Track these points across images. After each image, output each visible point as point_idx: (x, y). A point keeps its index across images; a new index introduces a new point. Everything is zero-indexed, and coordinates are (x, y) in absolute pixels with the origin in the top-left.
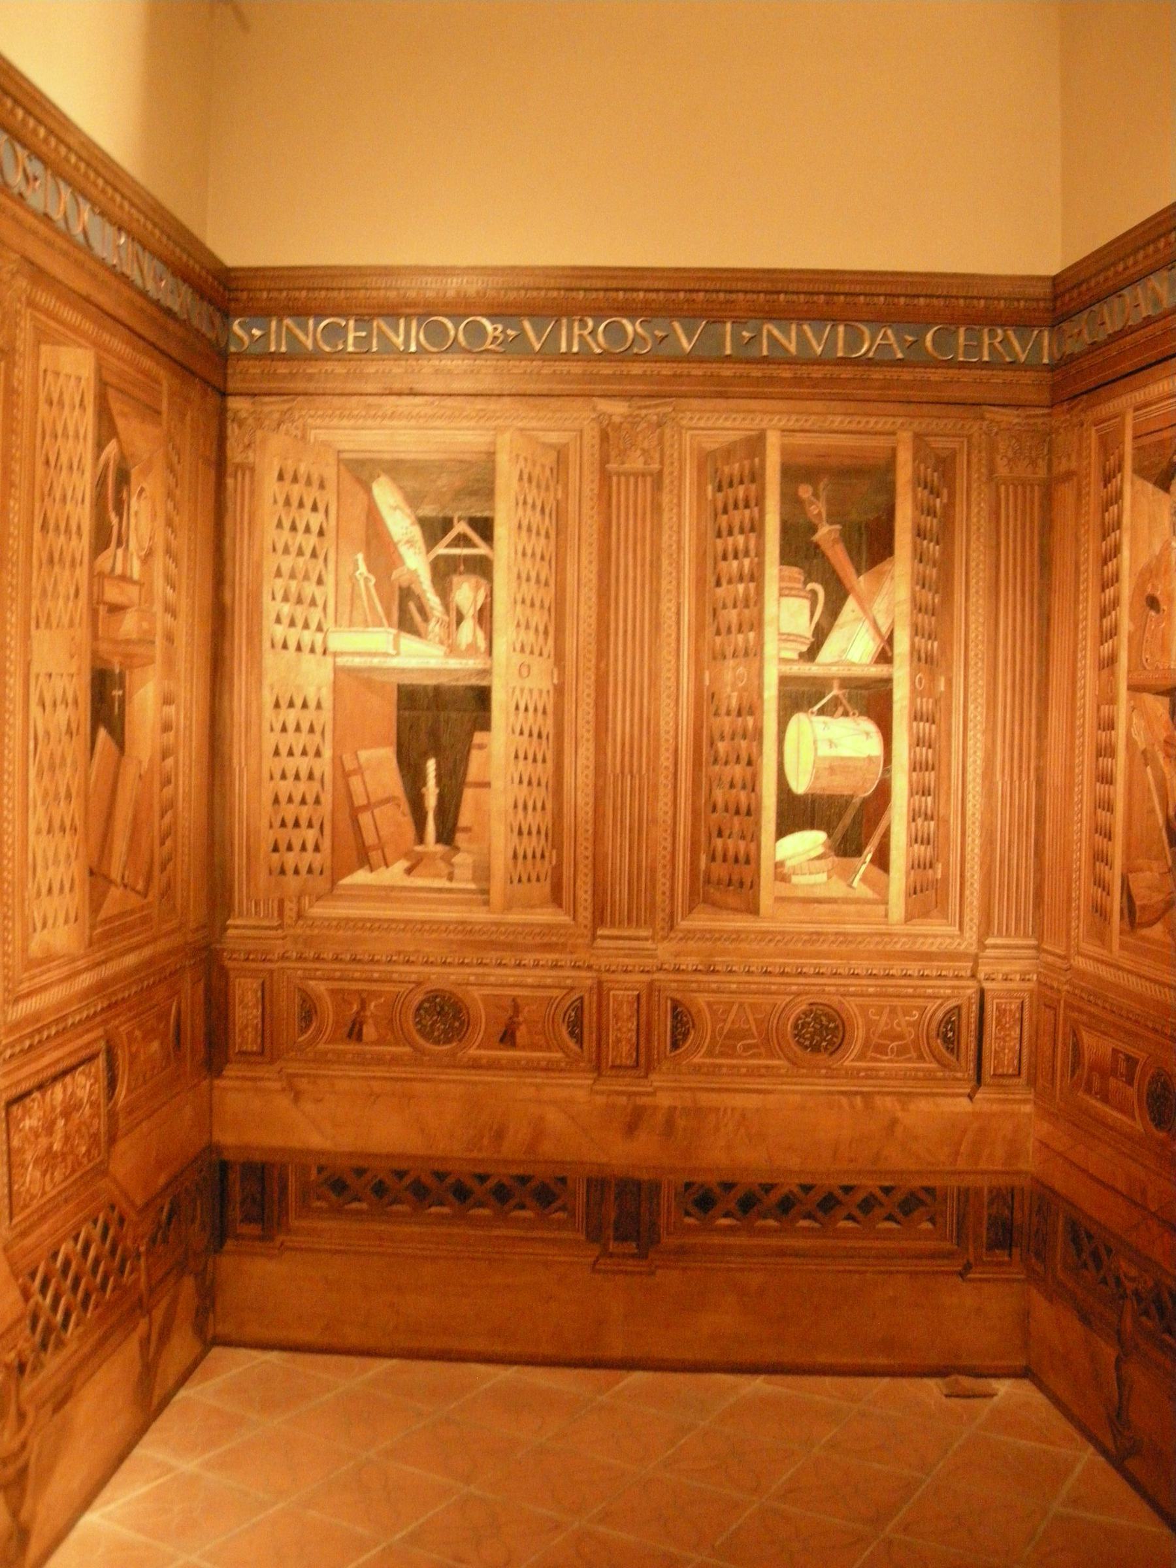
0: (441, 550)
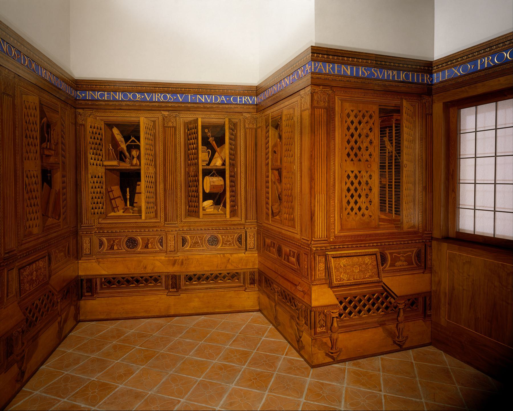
0: (128, 143)
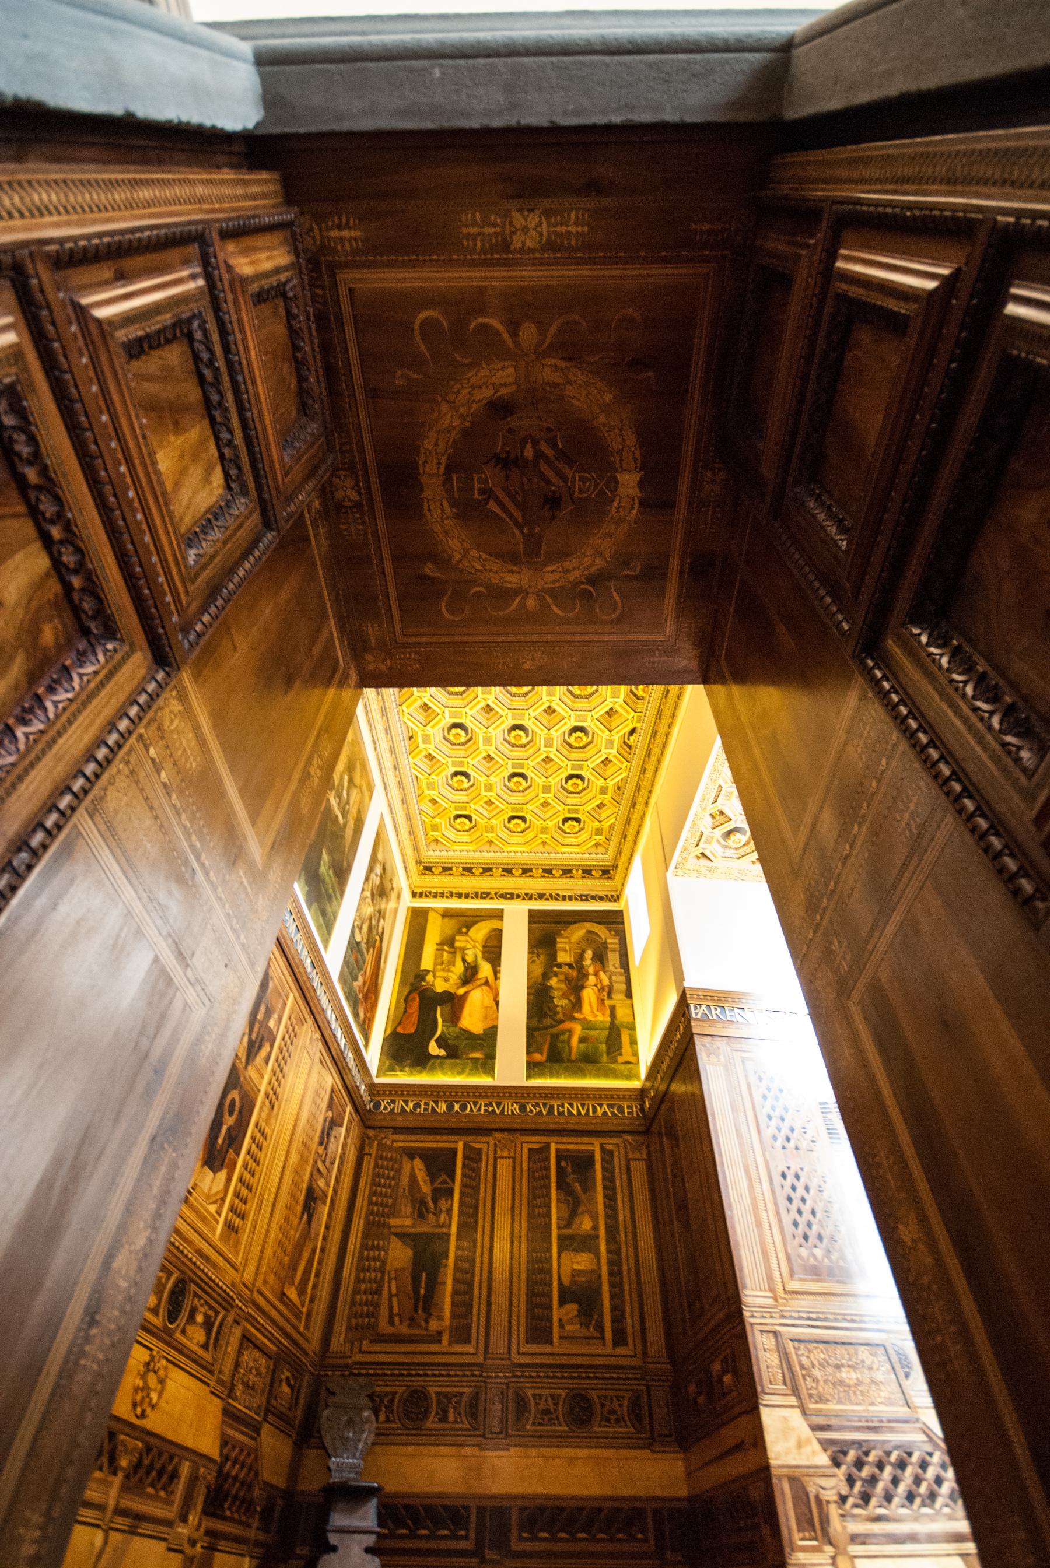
0: (437, 1184)
